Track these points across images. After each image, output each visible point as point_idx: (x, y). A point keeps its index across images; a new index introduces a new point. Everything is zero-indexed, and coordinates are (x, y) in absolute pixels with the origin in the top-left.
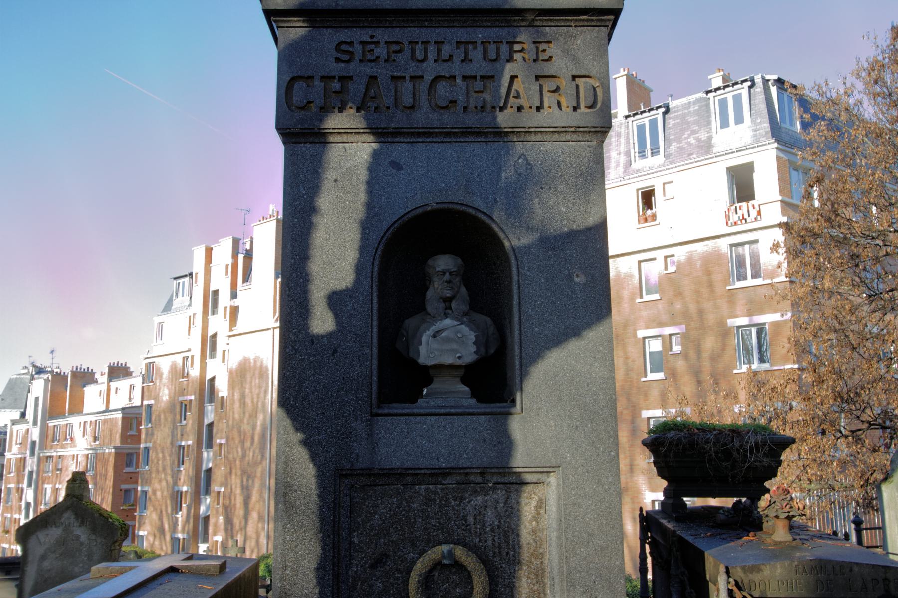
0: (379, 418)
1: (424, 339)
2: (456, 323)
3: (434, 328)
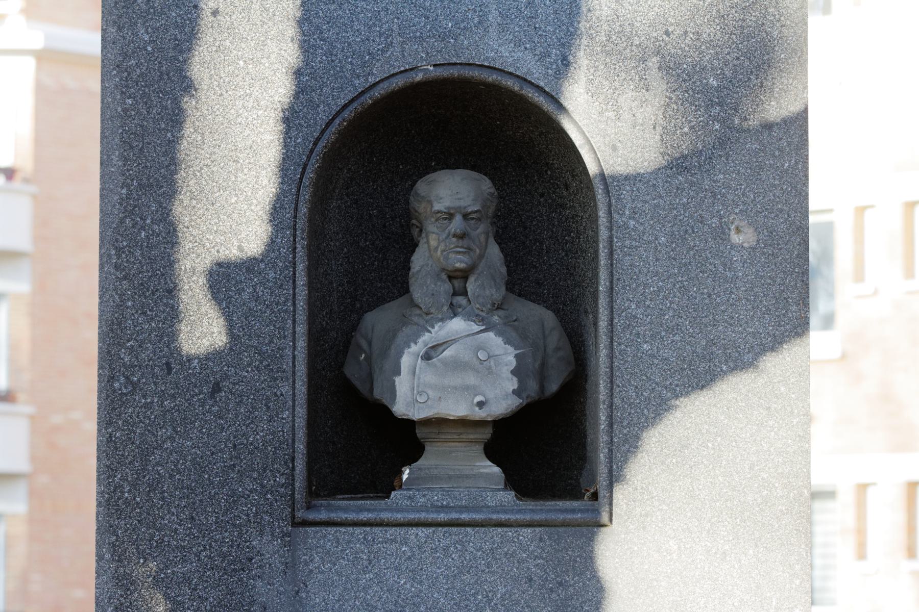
0: (310, 530)
1: (406, 361)
2: (476, 328)
3: (426, 339)
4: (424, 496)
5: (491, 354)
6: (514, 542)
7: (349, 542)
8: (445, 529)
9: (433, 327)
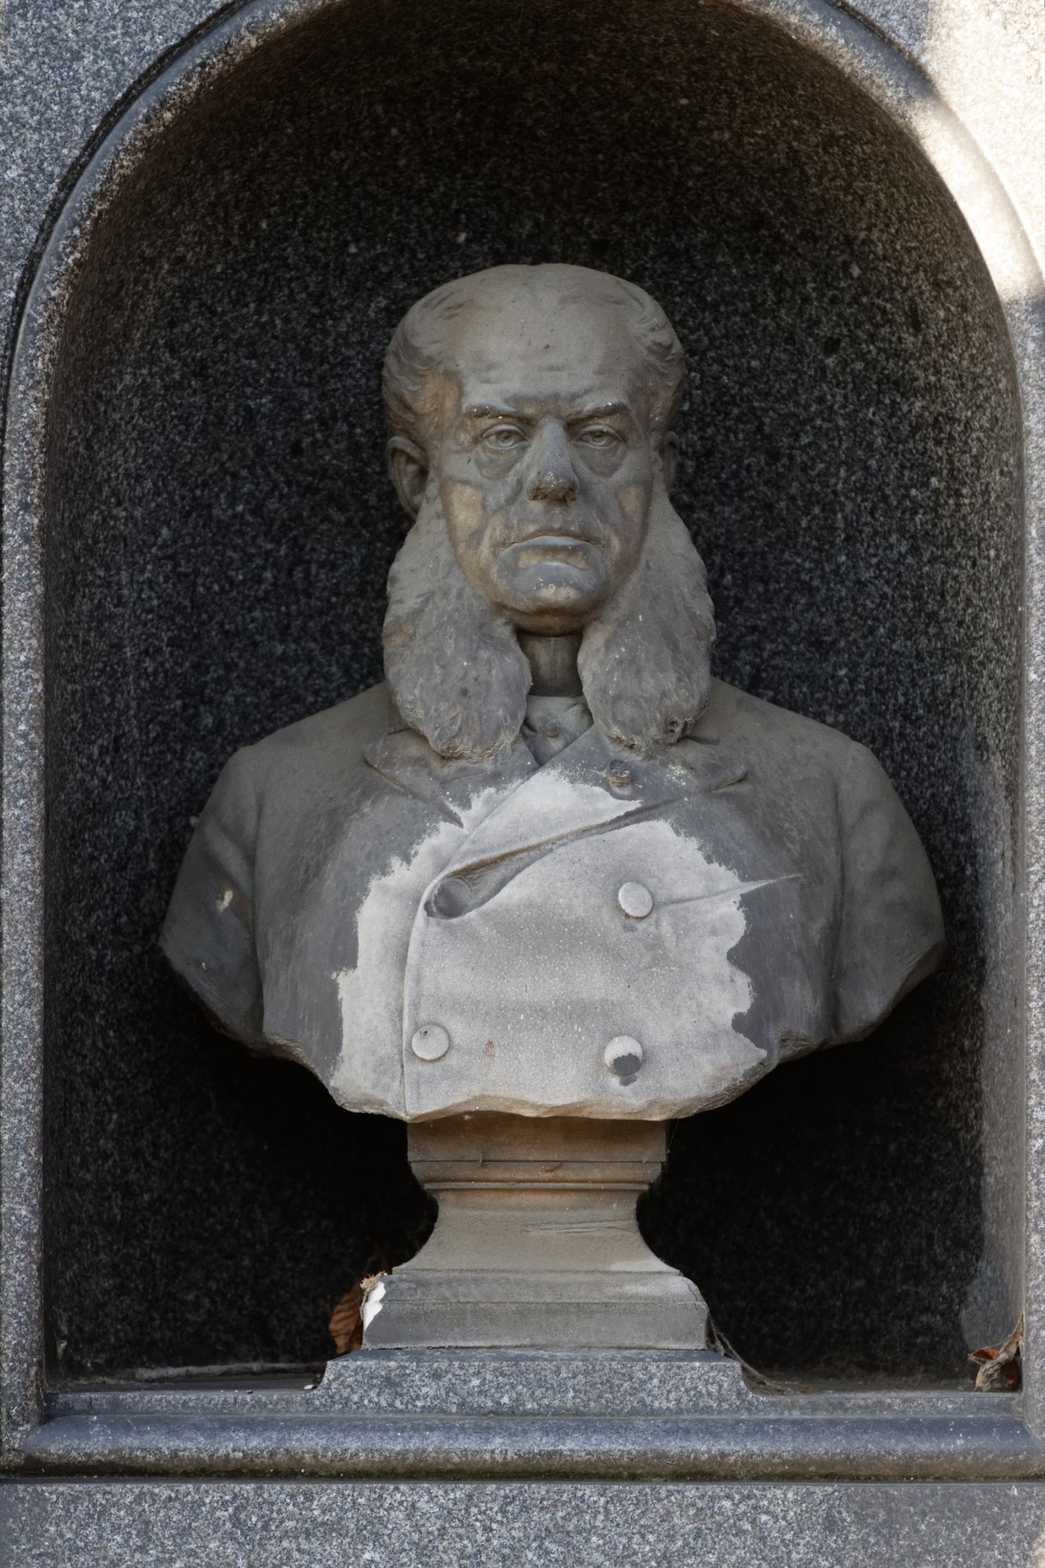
0: (54, 1491)
4: (436, 1376)
5: (662, 894)
6: (740, 1533)
7: (185, 1532)
8: (510, 1489)
9: (466, 804)
